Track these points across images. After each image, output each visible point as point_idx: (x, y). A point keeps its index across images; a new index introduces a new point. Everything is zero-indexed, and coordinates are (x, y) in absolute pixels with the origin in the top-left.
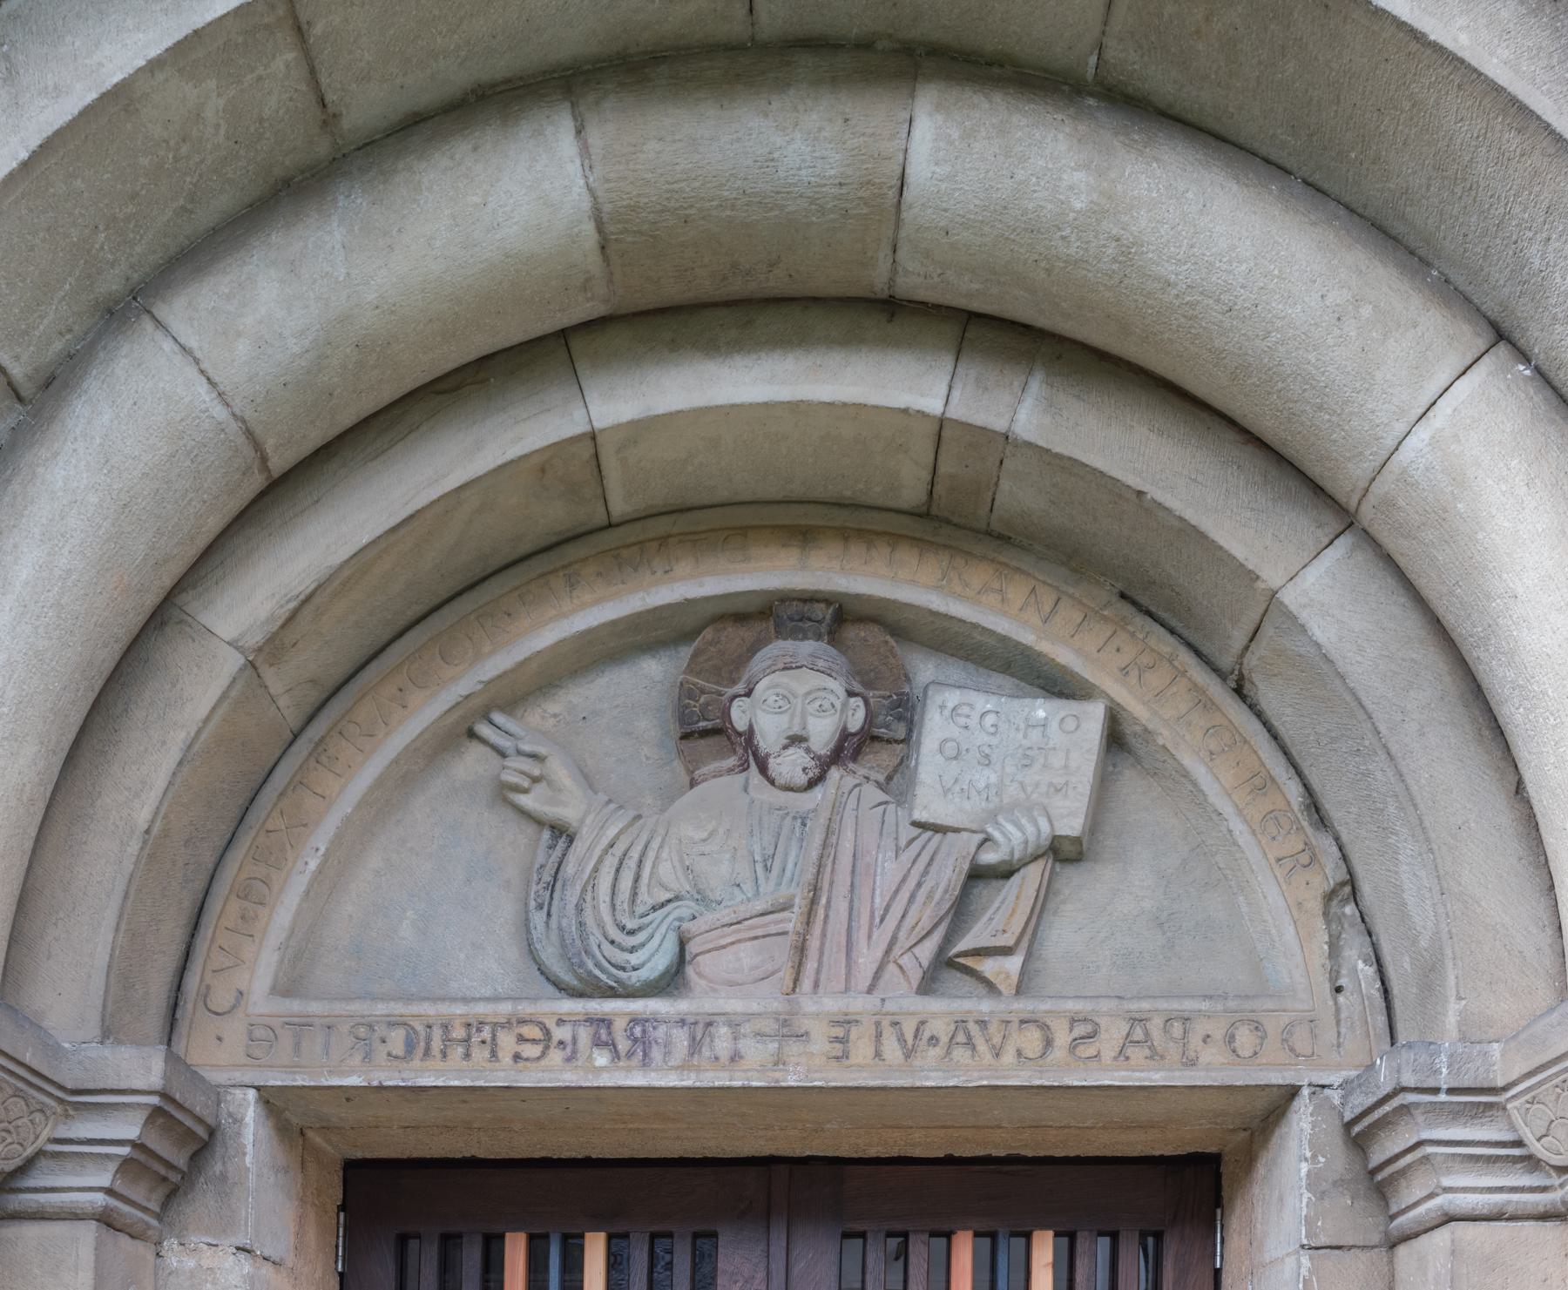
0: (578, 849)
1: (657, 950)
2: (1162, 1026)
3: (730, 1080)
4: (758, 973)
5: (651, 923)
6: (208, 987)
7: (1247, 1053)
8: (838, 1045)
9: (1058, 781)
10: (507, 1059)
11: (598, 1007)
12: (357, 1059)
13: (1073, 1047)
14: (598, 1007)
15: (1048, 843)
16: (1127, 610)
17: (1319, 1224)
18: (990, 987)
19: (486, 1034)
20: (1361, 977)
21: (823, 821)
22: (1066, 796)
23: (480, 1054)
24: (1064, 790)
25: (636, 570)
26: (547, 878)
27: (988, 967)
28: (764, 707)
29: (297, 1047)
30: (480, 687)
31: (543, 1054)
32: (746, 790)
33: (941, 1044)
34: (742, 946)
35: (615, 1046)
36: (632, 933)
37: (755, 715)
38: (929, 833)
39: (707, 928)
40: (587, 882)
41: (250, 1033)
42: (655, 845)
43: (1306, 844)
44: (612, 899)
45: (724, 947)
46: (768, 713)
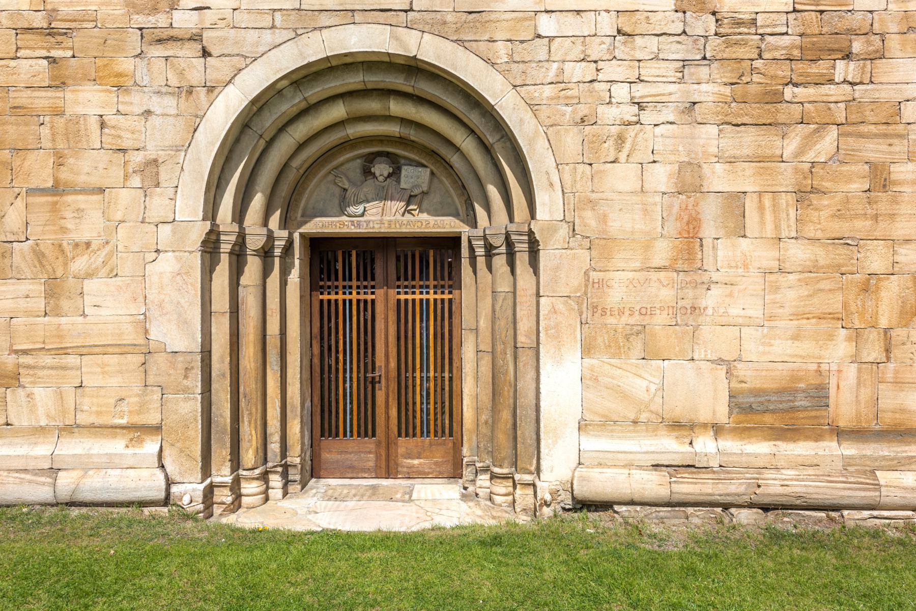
18: (414, 216)
23: (334, 227)
27: (413, 212)
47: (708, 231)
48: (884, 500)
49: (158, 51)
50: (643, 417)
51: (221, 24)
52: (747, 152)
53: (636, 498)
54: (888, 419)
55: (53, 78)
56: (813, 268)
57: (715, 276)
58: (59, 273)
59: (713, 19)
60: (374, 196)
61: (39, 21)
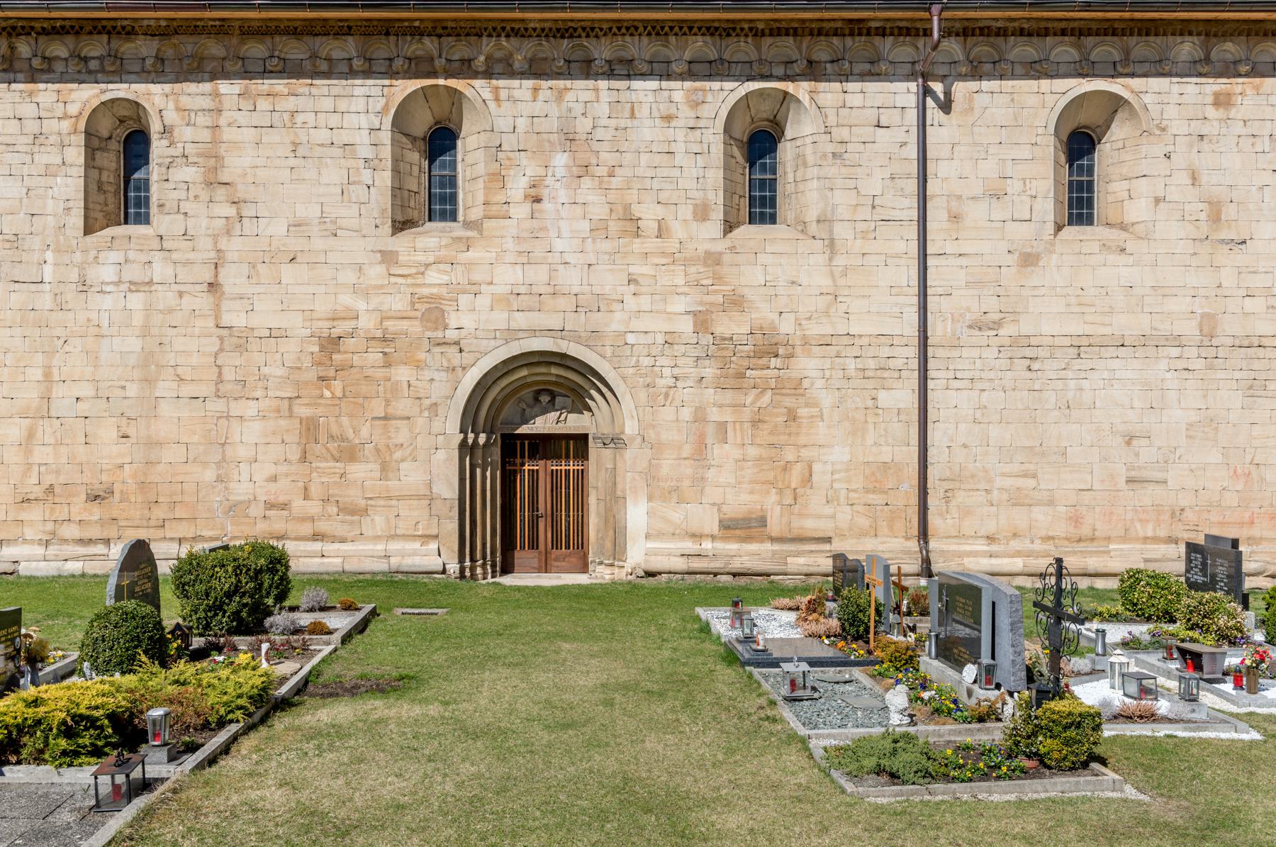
47: (709, 441)
48: (789, 570)
49: (439, 349)
50: (678, 532)
51: (469, 336)
52: (728, 402)
53: (672, 570)
54: (795, 533)
55: (385, 362)
56: (760, 459)
57: (713, 463)
58: (388, 459)
59: (711, 336)
61: (379, 334)
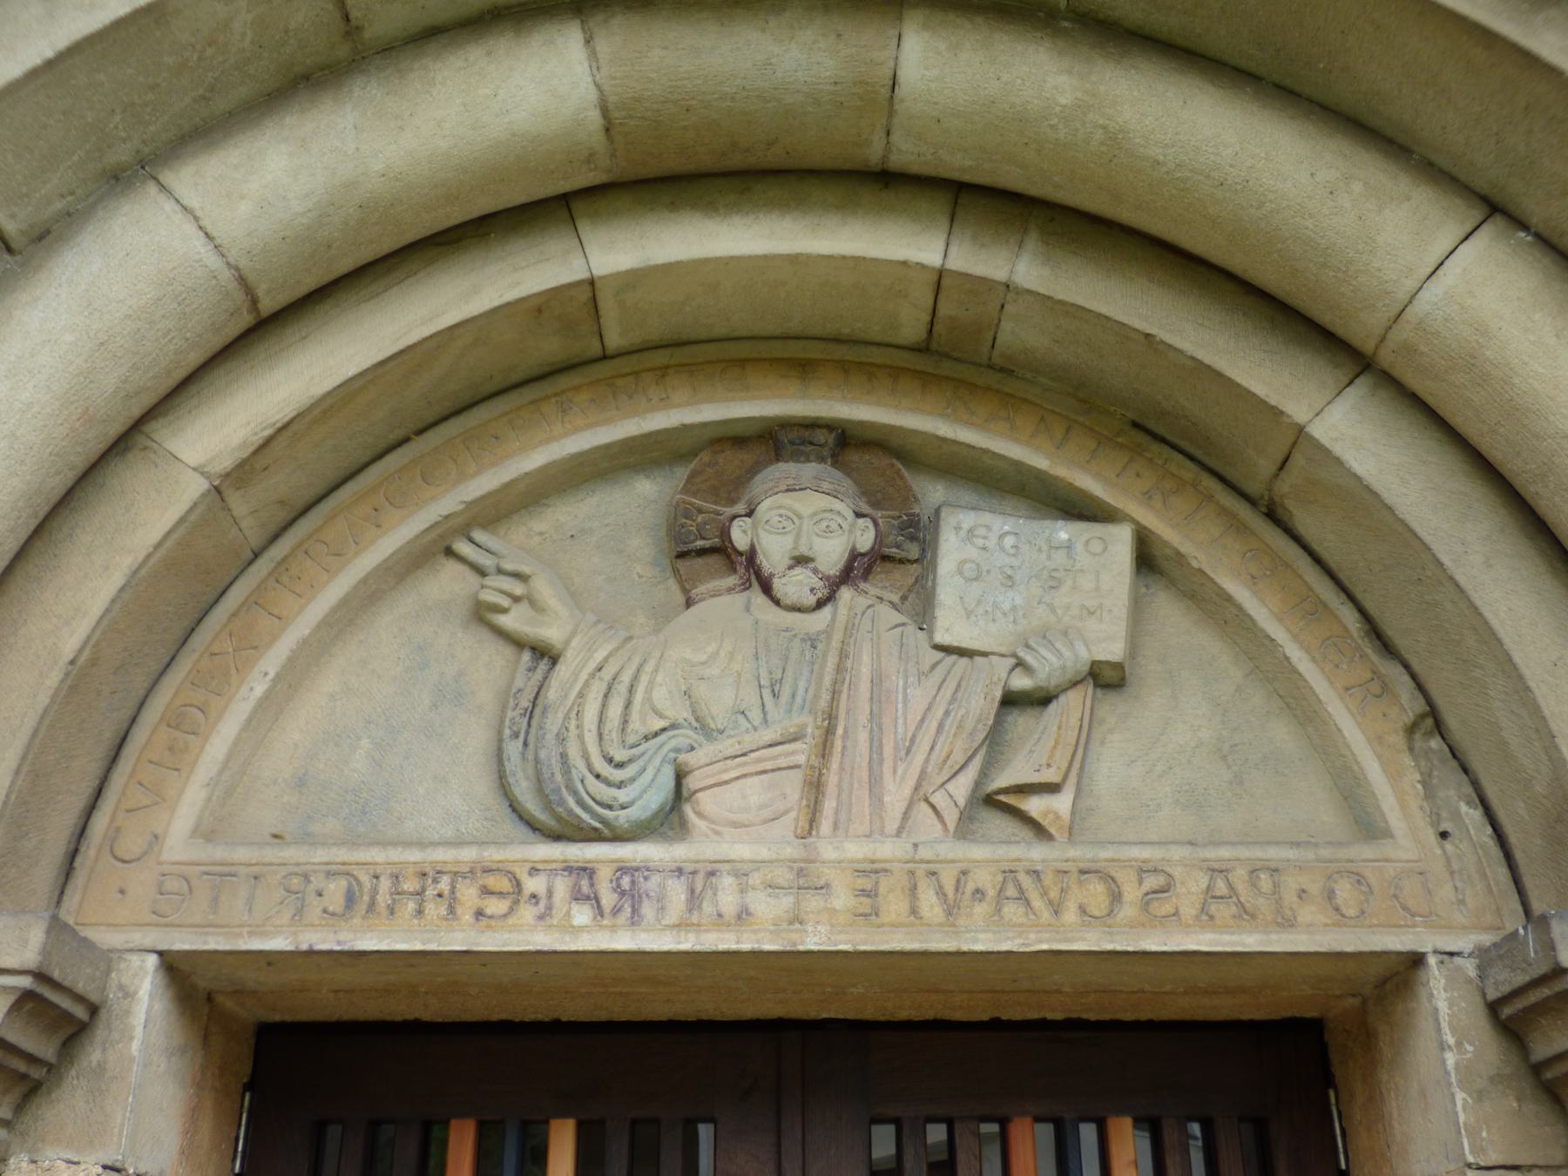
0: (562, 673)
1: (650, 786)
2: (1247, 878)
3: (738, 943)
4: (767, 813)
5: (643, 754)
6: (118, 829)
7: (1352, 912)
8: (863, 899)
9: (1090, 603)
10: (468, 917)
11: (579, 853)
12: (286, 916)
13: (1145, 906)
14: (579, 853)
15: (1087, 668)
16: (1142, 438)
17: (1484, 1134)
18: (1038, 830)
19: (444, 884)
20: (1467, 821)
21: (835, 643)
22: (1101, 619)
23: (434, 910)
24: (1099, 612)
25: (631, 397)
26: (525, 703)
27: (1034, 806)
28: (767, 527)
29: (215, 902)
30: (462, 507)
31: (511, 910)
32: (747, 609)
33: (988, 898)
34: (749, 781)
35: (598, 902)
36: (620, 765)
37: (757, 535)
38: (954, 657)
39: (708, 761)
40: (571, 709)
41: (161, 884)
42: (649, 668)
43: (1374, 673)
44: (599, 727)
45: (726, 782)
46: (771, 533)
60: (750, 698)
